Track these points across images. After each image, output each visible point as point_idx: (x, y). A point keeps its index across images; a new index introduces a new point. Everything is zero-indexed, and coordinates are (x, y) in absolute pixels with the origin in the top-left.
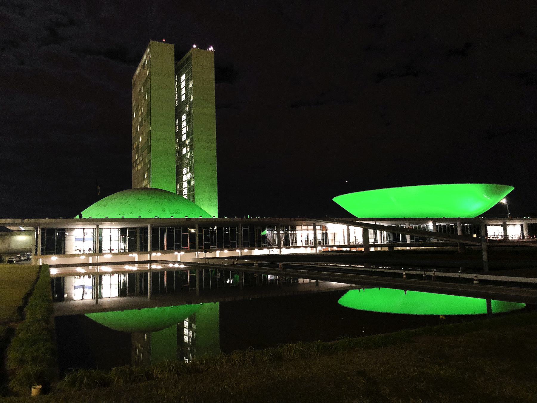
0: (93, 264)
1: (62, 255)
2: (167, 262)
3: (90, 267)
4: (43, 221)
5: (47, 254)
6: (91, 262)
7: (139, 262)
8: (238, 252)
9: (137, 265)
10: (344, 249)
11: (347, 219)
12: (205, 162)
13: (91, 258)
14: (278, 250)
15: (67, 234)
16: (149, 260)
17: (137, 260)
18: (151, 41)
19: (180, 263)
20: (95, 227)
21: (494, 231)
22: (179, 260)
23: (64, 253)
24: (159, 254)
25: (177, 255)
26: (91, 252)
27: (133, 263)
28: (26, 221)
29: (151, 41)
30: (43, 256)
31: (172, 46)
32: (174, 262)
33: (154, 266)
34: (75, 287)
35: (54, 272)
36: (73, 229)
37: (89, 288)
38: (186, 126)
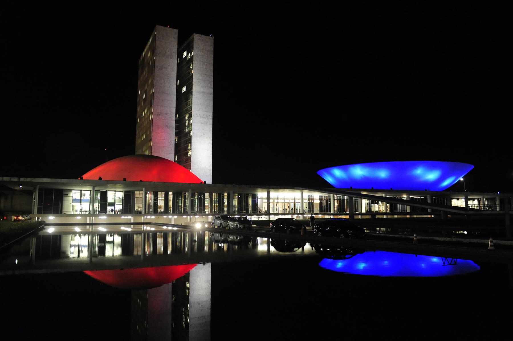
0: (90, 224)
1: (60, 215)
2: (163, 225)
3: (88, 227)
6: (88, 222)
7: (134, 224)
9: (132, 226)
13: (88, 218)
14: (267, 216)
16: (143, 222)
17: (132, 221)
19: (173, 226)
20: (91, 189)
22: (173, 223)
23: (61, 213)
24: (153, 217)
25: (171, 219)
26: (87, 213)
27: (128, 224)
30: (38, 215)
32: (168, 225)
33: (148, 228)
34: (71, 246)
35: (51, 230)
37: (84, 246)
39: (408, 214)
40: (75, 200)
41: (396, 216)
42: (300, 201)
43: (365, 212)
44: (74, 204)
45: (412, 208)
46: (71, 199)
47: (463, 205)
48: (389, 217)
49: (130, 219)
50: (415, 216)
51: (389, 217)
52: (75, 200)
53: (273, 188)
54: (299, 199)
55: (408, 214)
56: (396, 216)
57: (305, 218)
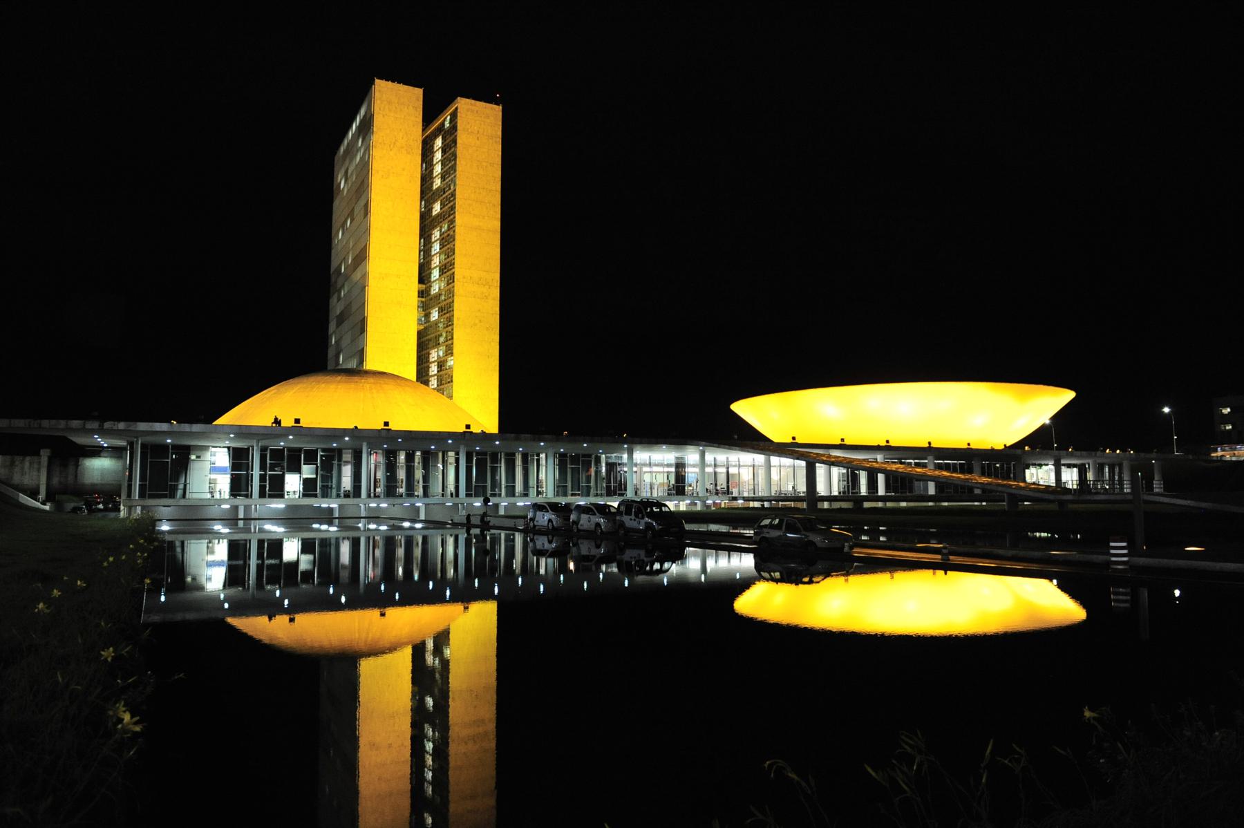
4: (142, 426)
5: (152, 496)
8: (1203, 505)
11: (762, 444)
15: (193, 457)
18: (377, 81)
21: (1041, 475)
24: (384, 505)
28: (107, 425)
29: (377, 81)
31: (419, 92)
36: (206, 448)
38: (440, 253)
39: (931, 498)
40: (215, 470)
41: (904, 504)
42: (697, 470)
43: (835, 493)
44: (213, 476)
45: (941, 485)
46: (208, 466)
47: (1052, 481)
48: (889, 504)
49: (331, 510)
50: (946, 504)
51: (889, 504)
52: (215, 470)
53: (641, 443)
54: (694, 466)
55: (931, 498)
56: (904, 504)
57: (708, 507)
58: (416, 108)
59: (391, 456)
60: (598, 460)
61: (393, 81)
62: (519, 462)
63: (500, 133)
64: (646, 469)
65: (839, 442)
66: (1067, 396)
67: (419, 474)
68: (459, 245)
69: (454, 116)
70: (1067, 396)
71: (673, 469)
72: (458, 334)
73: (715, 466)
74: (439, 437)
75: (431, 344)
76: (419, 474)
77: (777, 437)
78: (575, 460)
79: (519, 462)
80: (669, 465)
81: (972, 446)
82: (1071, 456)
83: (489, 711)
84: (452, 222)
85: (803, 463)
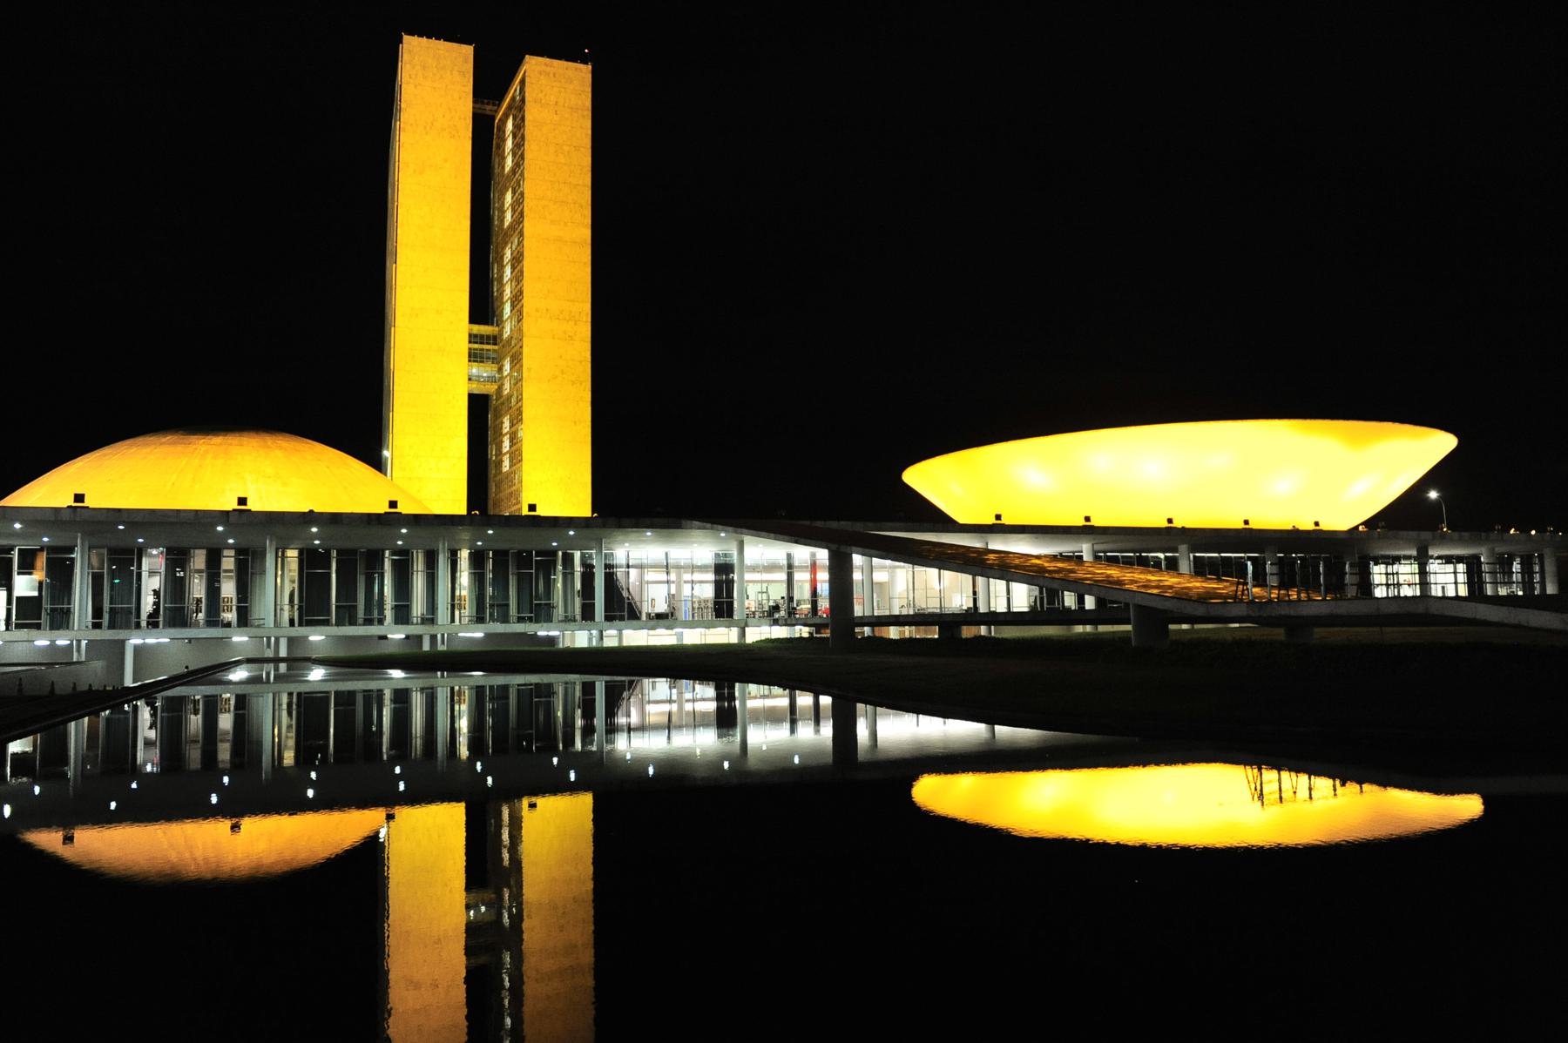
10: (893, 633)
12: (555, 377)
18: (406, 38)
29: (406, 38)
31: (468, 51)
58: (463, 73)
59: (177, 559)
60: (568, 560)
61: (429, 37)
62: (228, 563)
63: (588, 103)
64: (687, 577)
65: (991, 520)
66: (1441, 444)
67: (228, 589)
68: (528, 264)
69: (523, 82)
70: (1441, 444)
71: (711, 577)
72: (529, 391)
73: (790, 566)
74: (201, 520)
75: (505, 408)
76: (228, 589)
77: (962, 519)
78: (523, 559)
79: (228, 563)
80: (703, 568)
81: (1253, 525)
82: (1443, 540)
83: (582, 933)
84: (521, 234)
85: (823, 555)
